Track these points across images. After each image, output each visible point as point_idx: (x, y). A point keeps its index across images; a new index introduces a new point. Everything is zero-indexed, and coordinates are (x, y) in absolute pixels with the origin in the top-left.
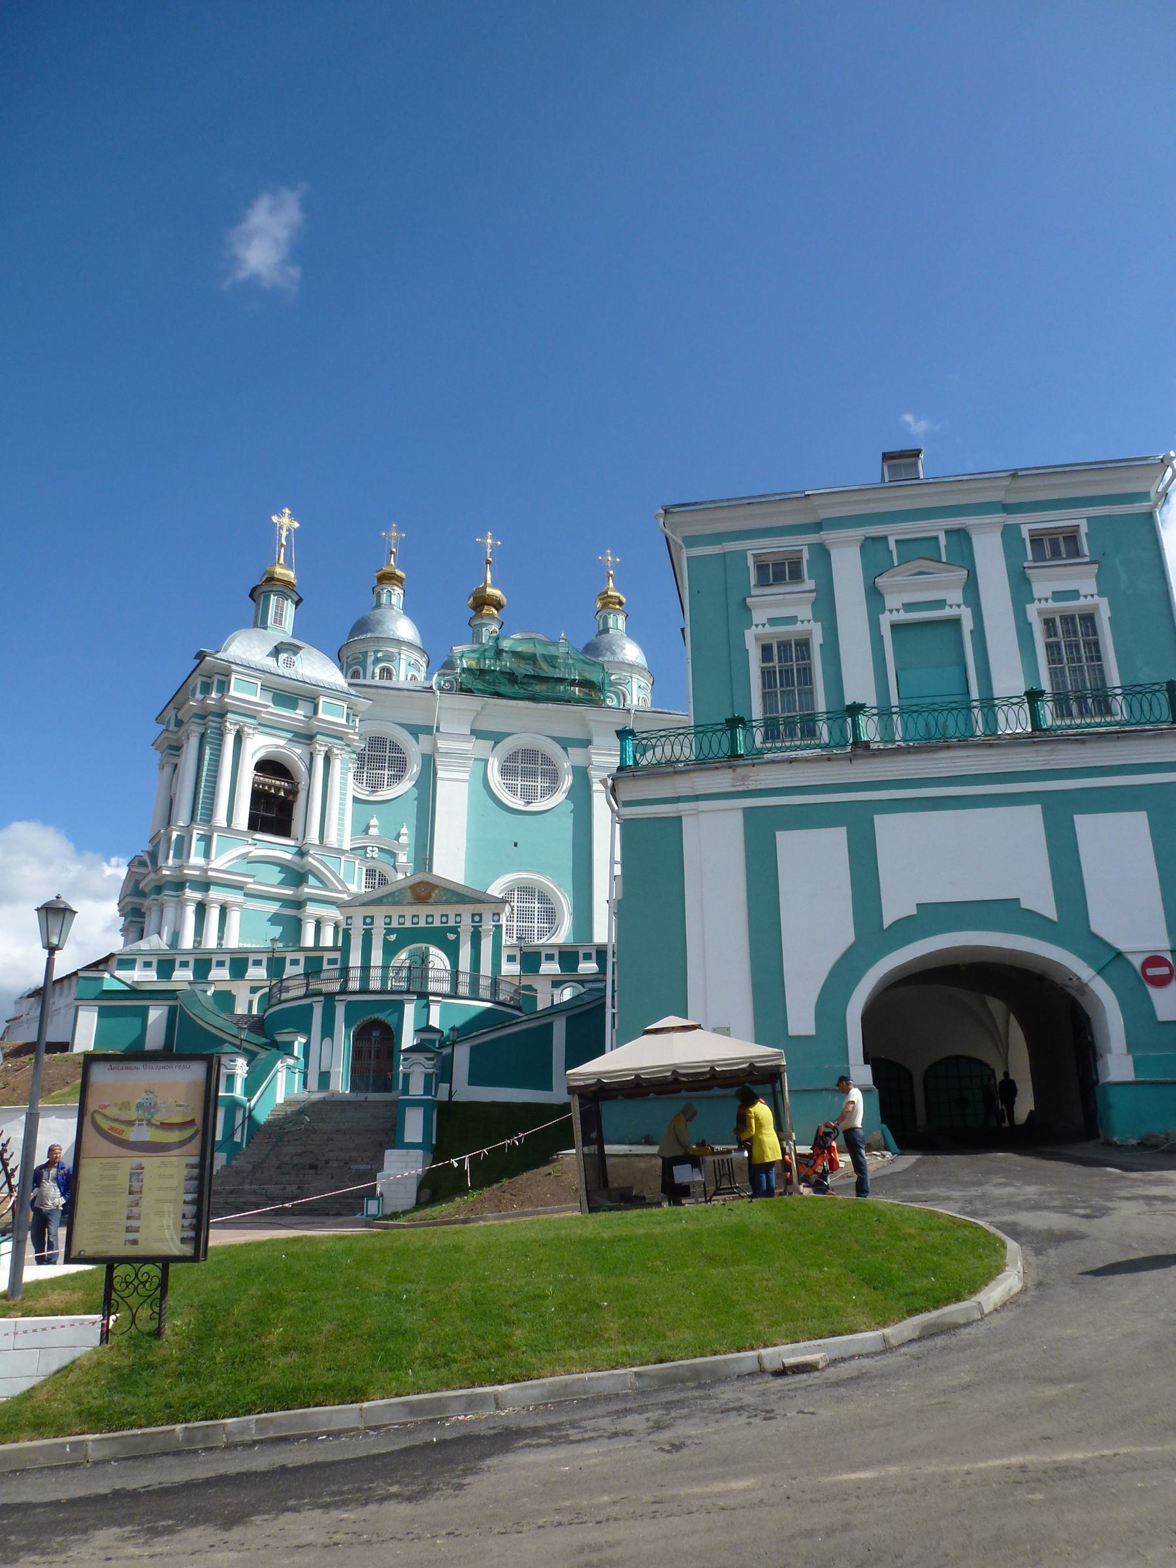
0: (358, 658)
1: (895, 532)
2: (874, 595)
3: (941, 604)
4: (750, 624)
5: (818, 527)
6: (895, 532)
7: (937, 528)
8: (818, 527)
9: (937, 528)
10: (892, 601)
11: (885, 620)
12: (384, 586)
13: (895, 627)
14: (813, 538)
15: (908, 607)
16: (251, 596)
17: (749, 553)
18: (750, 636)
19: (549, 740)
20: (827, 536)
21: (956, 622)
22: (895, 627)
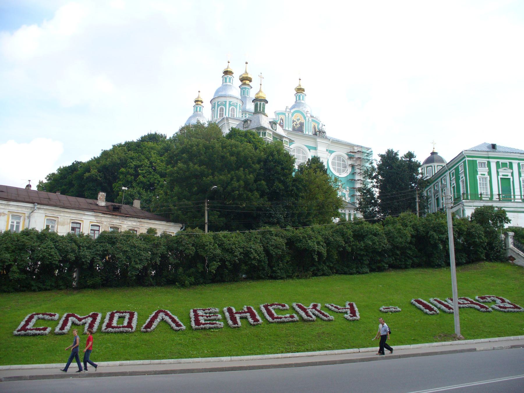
0: (223, 103)
1: (501, 161)
2: (498, 173)
3: (507, 176)
4: (477, 174)
5: (489, 158)
6: (501, 161)
7: (507, 161)
8: (489, 158)
9: (507, 161)
10: (500, 174)
11: (499, 177)
12: (228, 76)
13: (501, 178)
14: (488, 160)
15: (503, 175)
16: (253, 101)
17: (478, 161)
18: (478, 176)
19: (304, 146)
20: (490, 160)
21: (509, 179)
22: (501, 178)
